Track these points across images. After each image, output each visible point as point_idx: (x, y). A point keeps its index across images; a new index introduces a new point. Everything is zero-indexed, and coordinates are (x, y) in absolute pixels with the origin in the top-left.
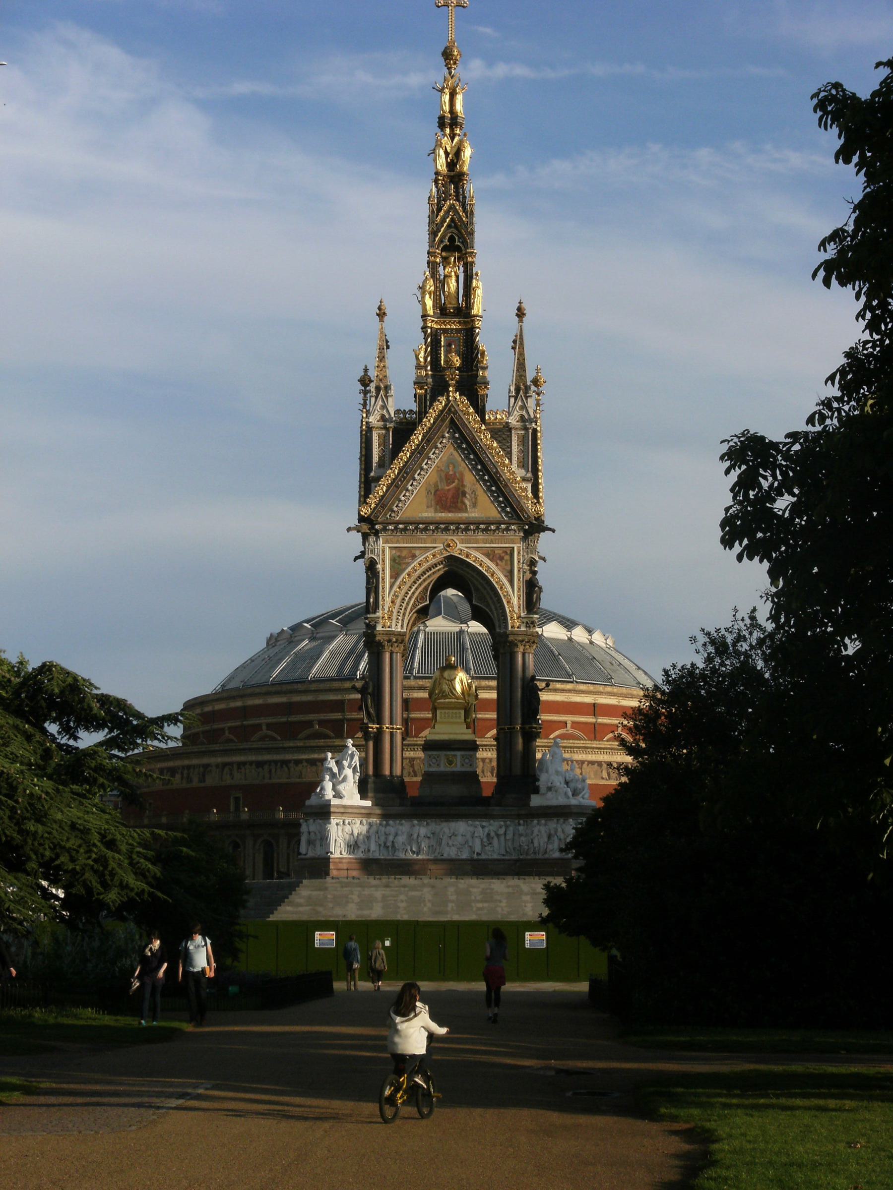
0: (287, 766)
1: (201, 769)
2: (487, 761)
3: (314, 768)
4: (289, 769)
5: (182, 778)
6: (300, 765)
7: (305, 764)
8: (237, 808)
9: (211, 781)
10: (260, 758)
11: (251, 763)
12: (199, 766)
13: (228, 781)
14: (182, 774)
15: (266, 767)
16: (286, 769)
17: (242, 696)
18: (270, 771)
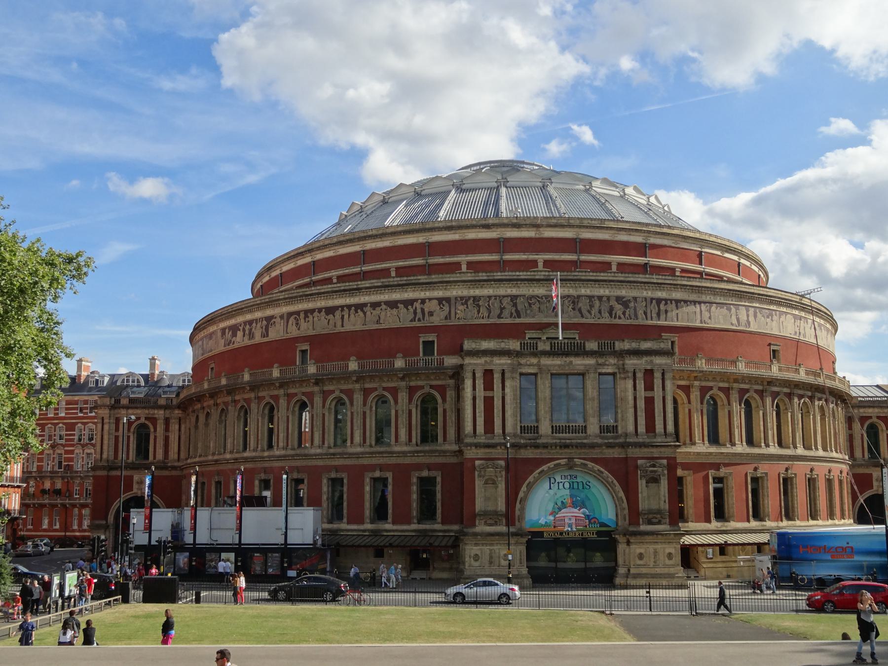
0: (362, 310)
1: (265, 322)
2: (605, 299)
3: (395, 311)
4: (365, 313)
5: (244, 336)
6: (377, 309)
7: (384, 307)
8: (304, 361)
9: (276, 333)
10: (331, 303)
11: (320, 310)
12: (261, 319)
13: (293, 332)
14: (244, 330)
15: (338, 314)
16: (360, 313)
17: (310, 251)
18: (343, 317)
